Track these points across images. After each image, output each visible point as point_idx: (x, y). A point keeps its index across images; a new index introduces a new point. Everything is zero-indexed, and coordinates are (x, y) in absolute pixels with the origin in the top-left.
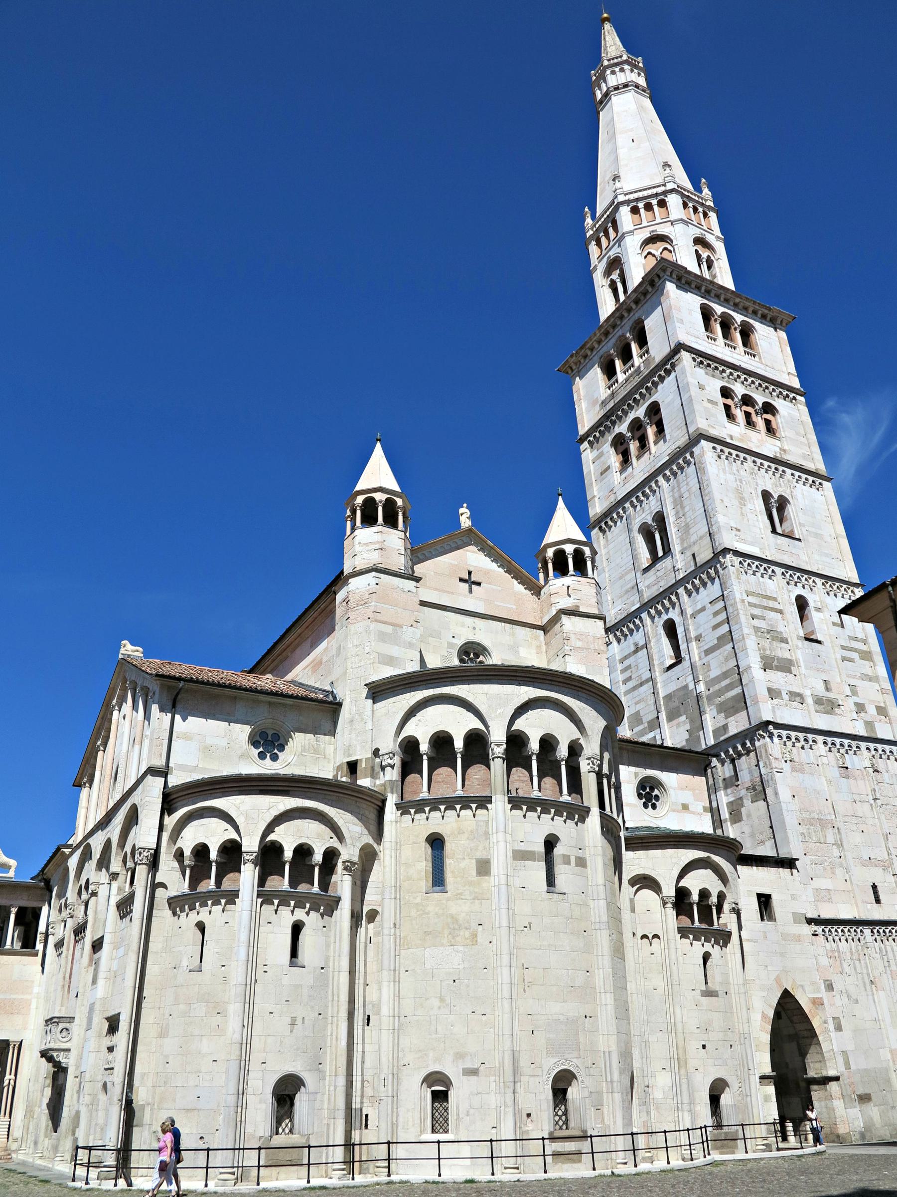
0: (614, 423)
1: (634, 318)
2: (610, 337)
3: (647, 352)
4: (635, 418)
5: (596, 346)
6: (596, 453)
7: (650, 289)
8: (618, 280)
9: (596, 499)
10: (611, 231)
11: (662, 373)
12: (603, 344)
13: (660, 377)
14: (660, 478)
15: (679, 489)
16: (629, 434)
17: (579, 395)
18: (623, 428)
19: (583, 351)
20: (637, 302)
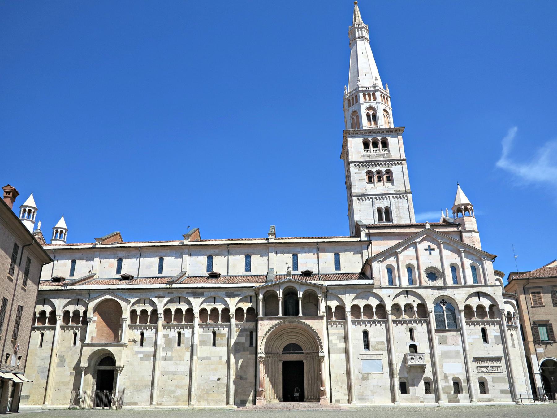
0: (369, 166)
1: (383, 135)
2: (371, 135)
3: (388, 150)
4: (379, 170)
5: (363, 133)
6: (357, 170)
7: (394, 132)
8: (371, 115)
9: (357, 187)
10: (371, 96)
11: (396, 163)
12: (367, 135)
13: (394, 163)
14: (391, 196)
15: (399, 204)
16: (375, 173)
17: (351, 145)
18: (374, 170)
19: (357, 132)
20: (387, 132)
